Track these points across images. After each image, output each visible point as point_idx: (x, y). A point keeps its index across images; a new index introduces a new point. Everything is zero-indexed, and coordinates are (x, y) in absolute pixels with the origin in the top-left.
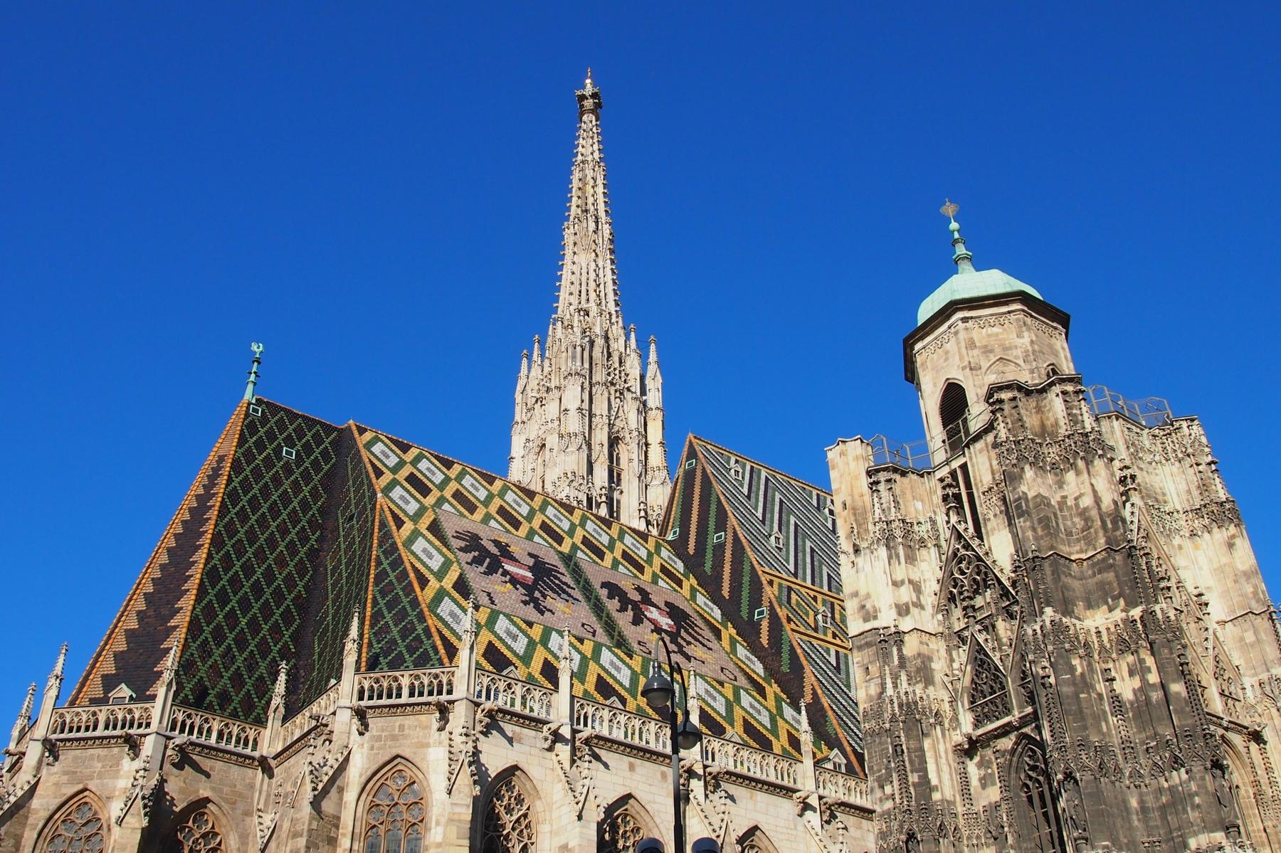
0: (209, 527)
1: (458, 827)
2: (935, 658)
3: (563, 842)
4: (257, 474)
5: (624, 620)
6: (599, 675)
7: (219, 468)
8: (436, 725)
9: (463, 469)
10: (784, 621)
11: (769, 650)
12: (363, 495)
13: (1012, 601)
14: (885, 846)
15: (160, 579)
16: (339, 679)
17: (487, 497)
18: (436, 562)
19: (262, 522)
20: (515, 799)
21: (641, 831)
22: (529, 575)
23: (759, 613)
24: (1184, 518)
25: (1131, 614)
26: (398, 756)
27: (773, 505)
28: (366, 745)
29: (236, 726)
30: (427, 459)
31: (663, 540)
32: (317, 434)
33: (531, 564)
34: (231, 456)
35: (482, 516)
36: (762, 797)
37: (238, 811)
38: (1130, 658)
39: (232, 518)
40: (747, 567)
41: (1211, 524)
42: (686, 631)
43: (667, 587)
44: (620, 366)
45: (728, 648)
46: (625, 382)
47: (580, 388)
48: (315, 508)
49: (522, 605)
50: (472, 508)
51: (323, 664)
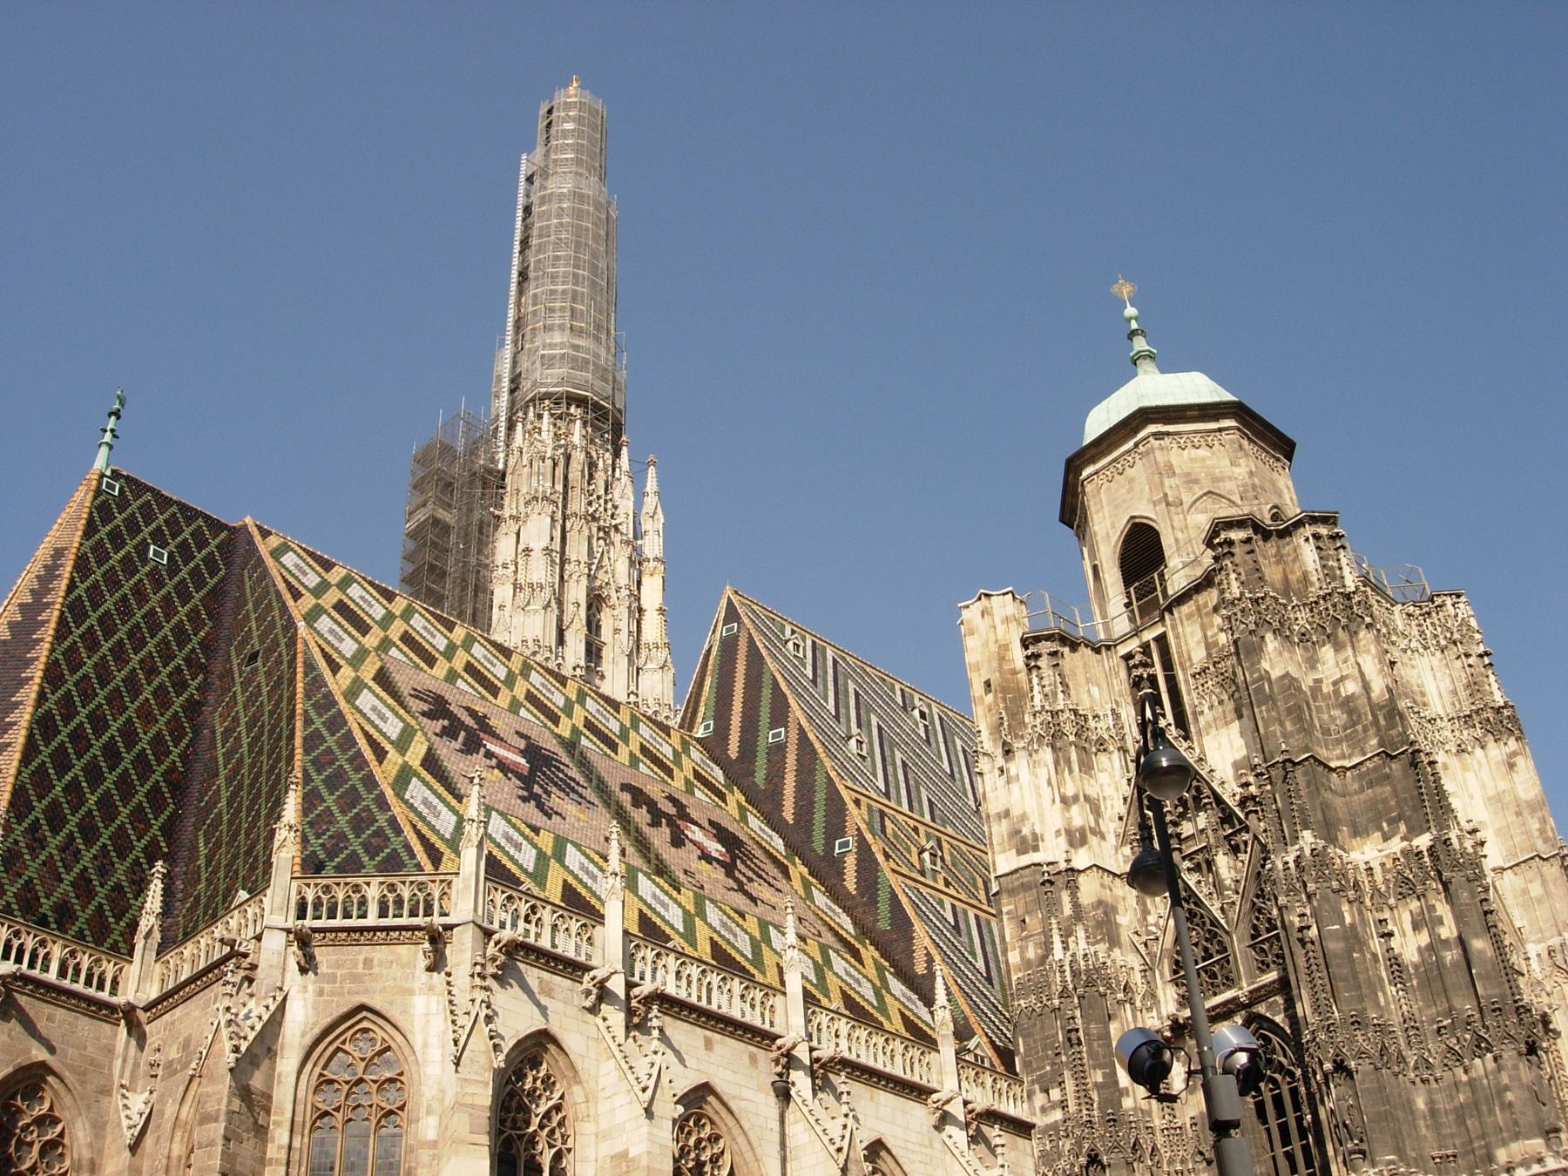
0: (42, 652)
1: (471, 1115)
2: (1121, 909)
3: (618, 1148)
4: (113, 582)
5: (660, 838)
6: (640, 911)
7: (55, 567)
8: (423, 963)
9: (410, 605)
10: (880, 858)
11: (858, 899)
12: (273, 624)
13: (1238, 827)
16: (257, 888)
17: (448, 647)
18: (393, 728)
19: (119, 652)
20: (543, 1082)
21: (722, 1141)
22: (523, 761)
23: (842, 845)
24: (1450, 728)
25: (1415, 842)
26: (363, 1007)
27: (847, 696)
28: (310, 988)
29: (87, 956)
31: (690, 737)
32: (199, 530)
33: (522, 747)
34: (74, 551)
35: (445, 672)
38: (1414, 905)
39: (75, 642)
40: (820, 779)
41: (1485, 736)
42: (744, 862)
43: (707, 799)
44: (606, 493)
45: (801, 891)
46: (612, 516)
47: (549, 520)
48: (195, 640)
49: (519, 801)
50: (431, 661)
51: (215, 872)
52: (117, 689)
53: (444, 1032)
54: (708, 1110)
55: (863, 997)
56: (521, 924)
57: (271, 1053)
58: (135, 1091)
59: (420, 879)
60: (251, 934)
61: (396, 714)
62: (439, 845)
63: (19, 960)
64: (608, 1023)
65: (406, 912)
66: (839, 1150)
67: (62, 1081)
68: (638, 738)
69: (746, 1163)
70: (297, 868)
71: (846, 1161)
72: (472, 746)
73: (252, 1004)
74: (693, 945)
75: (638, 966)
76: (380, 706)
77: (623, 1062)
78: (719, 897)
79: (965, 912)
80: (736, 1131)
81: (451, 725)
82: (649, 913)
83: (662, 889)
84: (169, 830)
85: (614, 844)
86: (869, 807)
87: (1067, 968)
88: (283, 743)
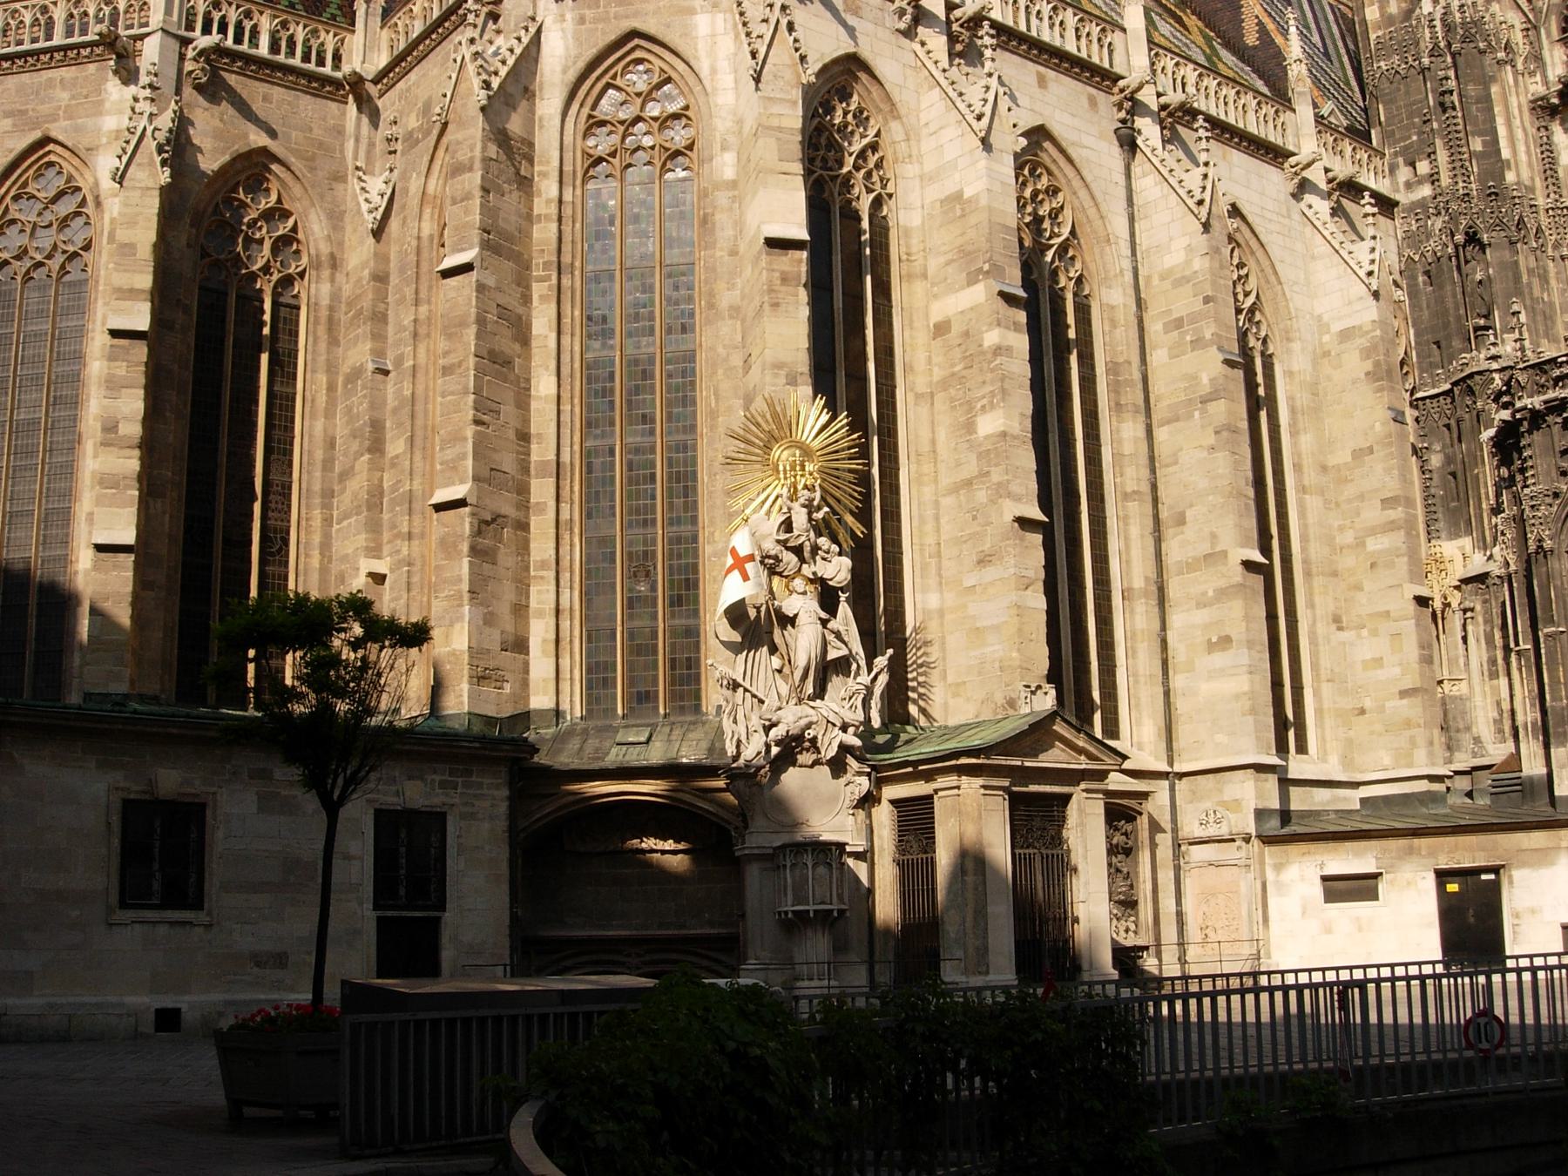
1: (778, 139)
3: (950, 188)
14: (1416, 258)
20: (855, 116)
21: (1061, 195)
26: (634, 34)
28: (569, 16)
29: (301, 27)
37: (320, 174)
54: (1044, 158)
57: (529, 93)
58: (372, 174)
66: (1200, 203)
67: (289, 169)
69: (1089, 221)
71: (1209, 214)
73: (500, 41)
87: (1438, 23)
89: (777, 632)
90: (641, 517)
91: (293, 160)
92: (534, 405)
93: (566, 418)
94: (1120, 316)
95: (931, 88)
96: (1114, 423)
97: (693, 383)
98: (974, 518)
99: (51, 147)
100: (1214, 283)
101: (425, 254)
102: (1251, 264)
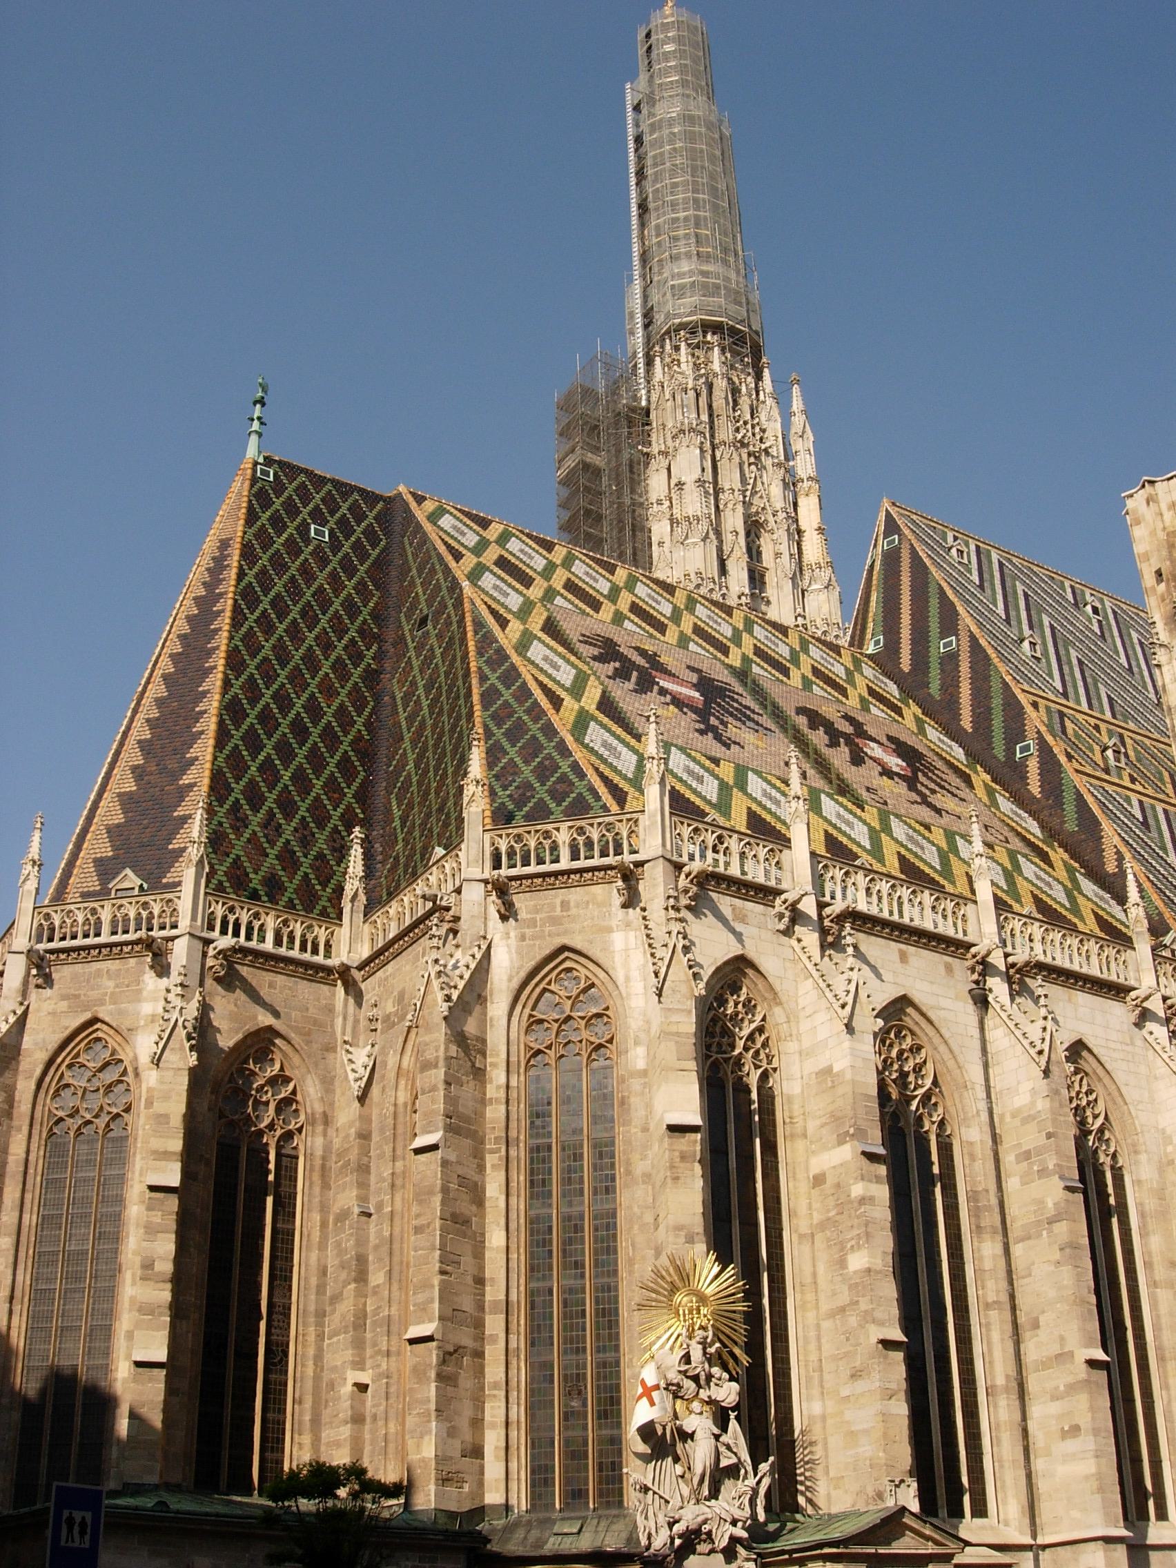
0: (222, 640)
1: (677, 1042)
3: (822, 1064)
4: (279, 564)
5: (839, 757)
6: (826, 831)
8: (617, 900)
10: (1063, 759)
12: (438, 587)
15: (158, 719)
16: (452, 844)
17: (611, 590)
18: (566, 675)
20: (744, 1006)
21: (923, 1051)
22: (697, 695)
26: (564, 948)
27: (1016, 599)
28: (512, 934)
29: (299, 924)
30: (517, 537)
31: (861, 654)
33: (695, 680)
34: (239, 540)
35: (611, 615)
36: (1084, 1000)
37: (315, 1046)
39: (252, 628)
40: (996, 686)
42: (925, 775)
43: (883, 715)
44: (752, 417)
45: (985, 799)
46: (761, 440)
47: (698, 451)
48: (365, 611)
49: (696, 734)
50: (596, 606)
51: (410, 832)
52: (297, 668)
53: (644, 966)
54: (908, 1021)
55: (1054, 899)
56: (710, 854)
57: (482, 999)
58: (358, 1046)
59: (607, 819)
60: (450, 888)
61: (568, 661)
62: (623, 785)
63: (236, 934)
64: (803, 944)
65: (596, 853)
66: (1040, 1052)
67: (289, 1043)
68: (810, 661)
69: (949, 1071)
70: (488, 820)
71: (1048, 1062)
72: (645, 685)
73: (458, 954)
74: (881, 860)
75: (828, 887)
76: (551, 655)
77: (820, 981)
78: (903, 812)
79: (1153, 808)
80: (937, 1040)
81: (623, 666)
82: (835, 833)
83: (846, 808)
84: (363, 796)
85: (794, 767)
86: (1048, 708)
88: (462, 701)
89: (679, 1447)
90: (574, 1346)
91: (293, 1035)
92: (488, 1255)
93: (513, 1264)
94: (978, 1150)
95: (806, 978)
96: (976, 1244)
97: (615, 1236)
98: (848, 1339)
99: (98, 1025)
100: (1054, 1121)
101: (401, 1119)
102: (1099, 1089)
